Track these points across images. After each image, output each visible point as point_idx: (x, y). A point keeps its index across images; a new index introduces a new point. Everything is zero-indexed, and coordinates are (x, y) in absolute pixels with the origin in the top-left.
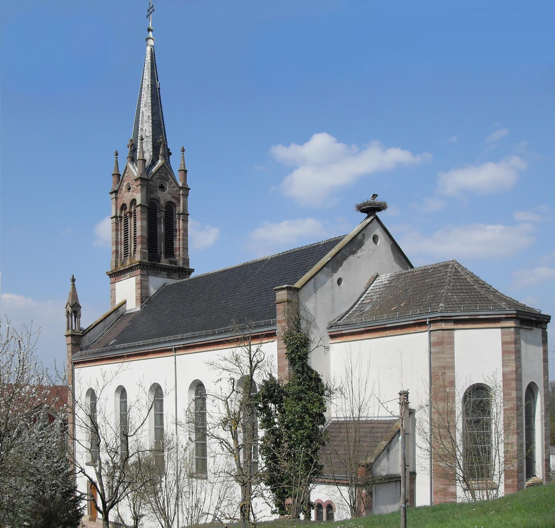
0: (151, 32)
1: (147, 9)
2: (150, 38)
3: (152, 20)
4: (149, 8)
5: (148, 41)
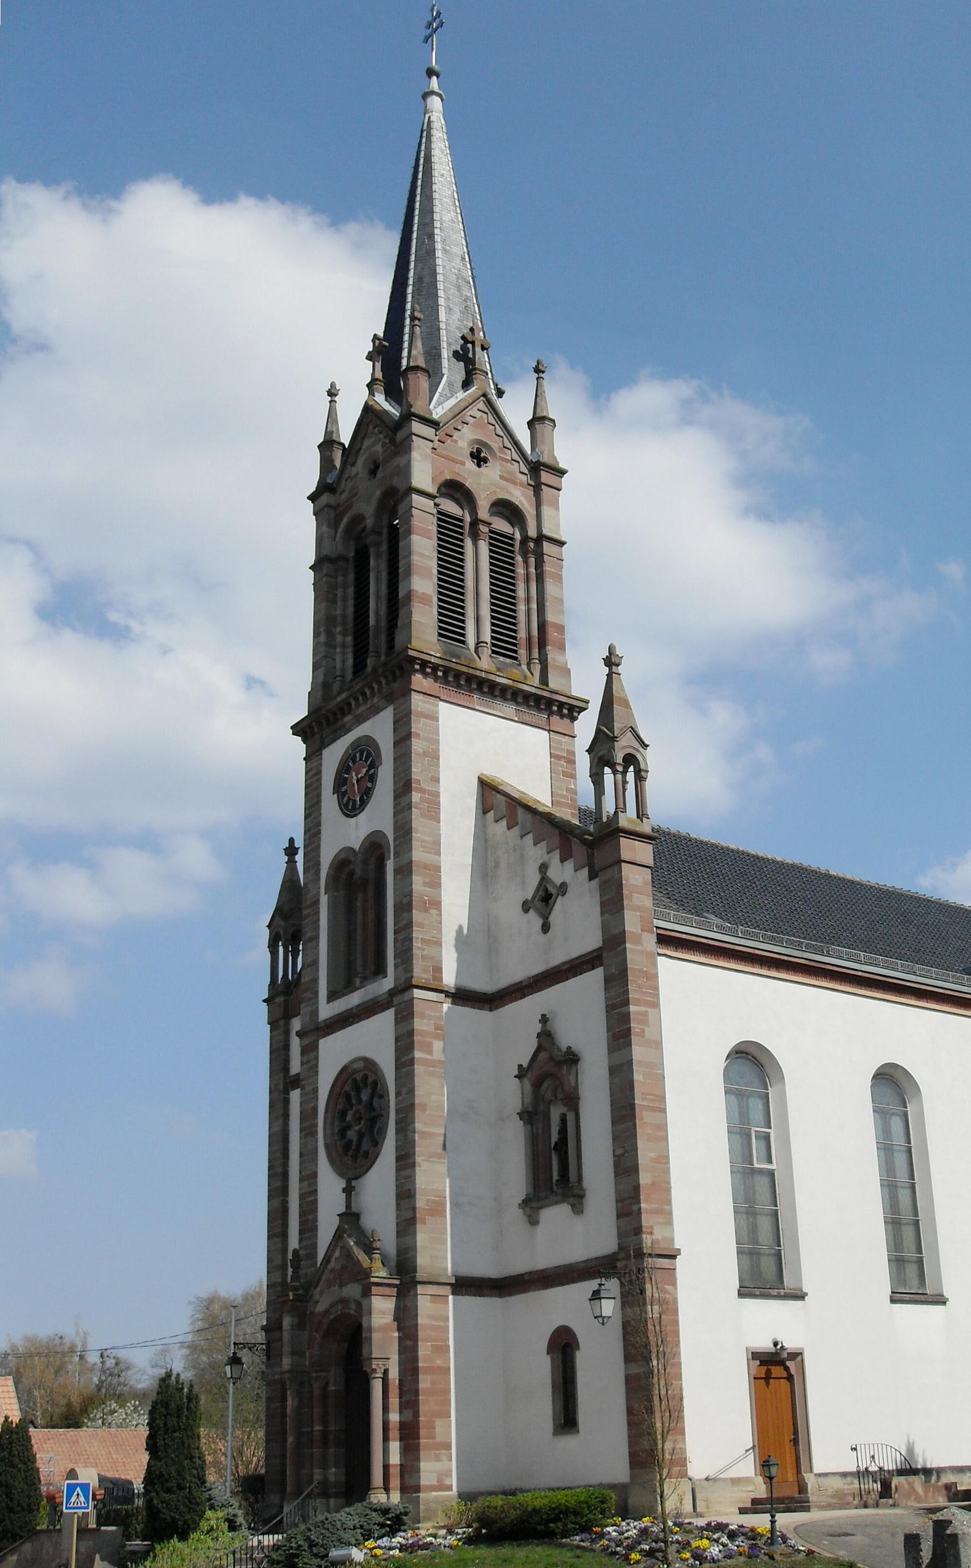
0: (434, 78)
1: (427, 22)
2: (433, 93)
3: (437, 48)
4: (430, 19)
5: (429, 100)
